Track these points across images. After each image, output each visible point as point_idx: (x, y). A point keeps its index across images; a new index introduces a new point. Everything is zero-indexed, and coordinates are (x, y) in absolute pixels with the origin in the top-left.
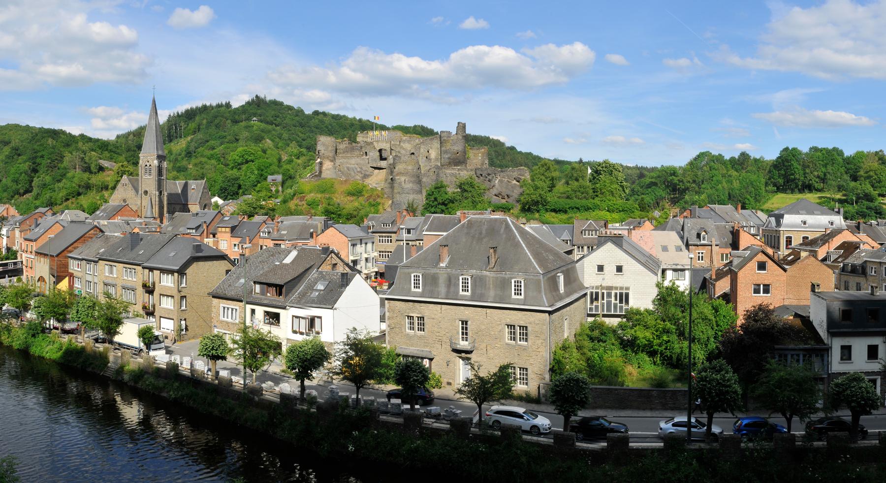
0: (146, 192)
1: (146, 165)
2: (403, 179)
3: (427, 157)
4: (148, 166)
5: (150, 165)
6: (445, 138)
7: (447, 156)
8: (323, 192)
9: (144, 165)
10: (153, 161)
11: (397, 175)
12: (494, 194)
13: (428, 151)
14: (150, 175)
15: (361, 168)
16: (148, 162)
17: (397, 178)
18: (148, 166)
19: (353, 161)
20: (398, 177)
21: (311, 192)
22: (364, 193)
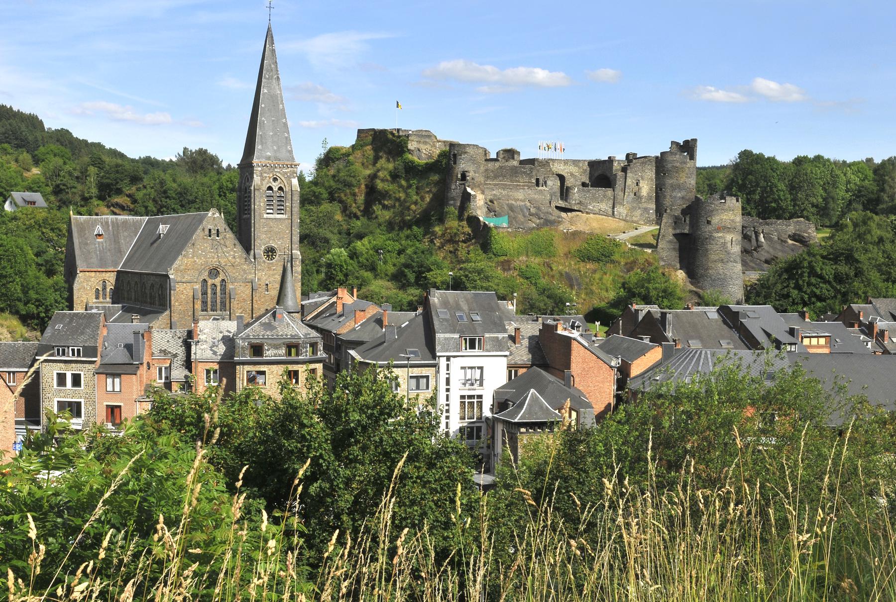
0: (270, 252)
1: (270, 188)
2: (729, 237)
3: (635, 195)
4: (275, 189)
5: (280, 189)
6: (678, 165)
7: (679, 195)
8: (538, 253)
9: (265, 187)
10: (289, 178)
11: (718, 230)
12: (763, 259)
13: (637, 184)
14: (280, 211)
15: (538, 208)
16: (275, 180)
17: (716, 235)
18: (275, 189)
19: (520, 195)
20: (720, 235)
21: (519, 254)
22: (616, 257)
